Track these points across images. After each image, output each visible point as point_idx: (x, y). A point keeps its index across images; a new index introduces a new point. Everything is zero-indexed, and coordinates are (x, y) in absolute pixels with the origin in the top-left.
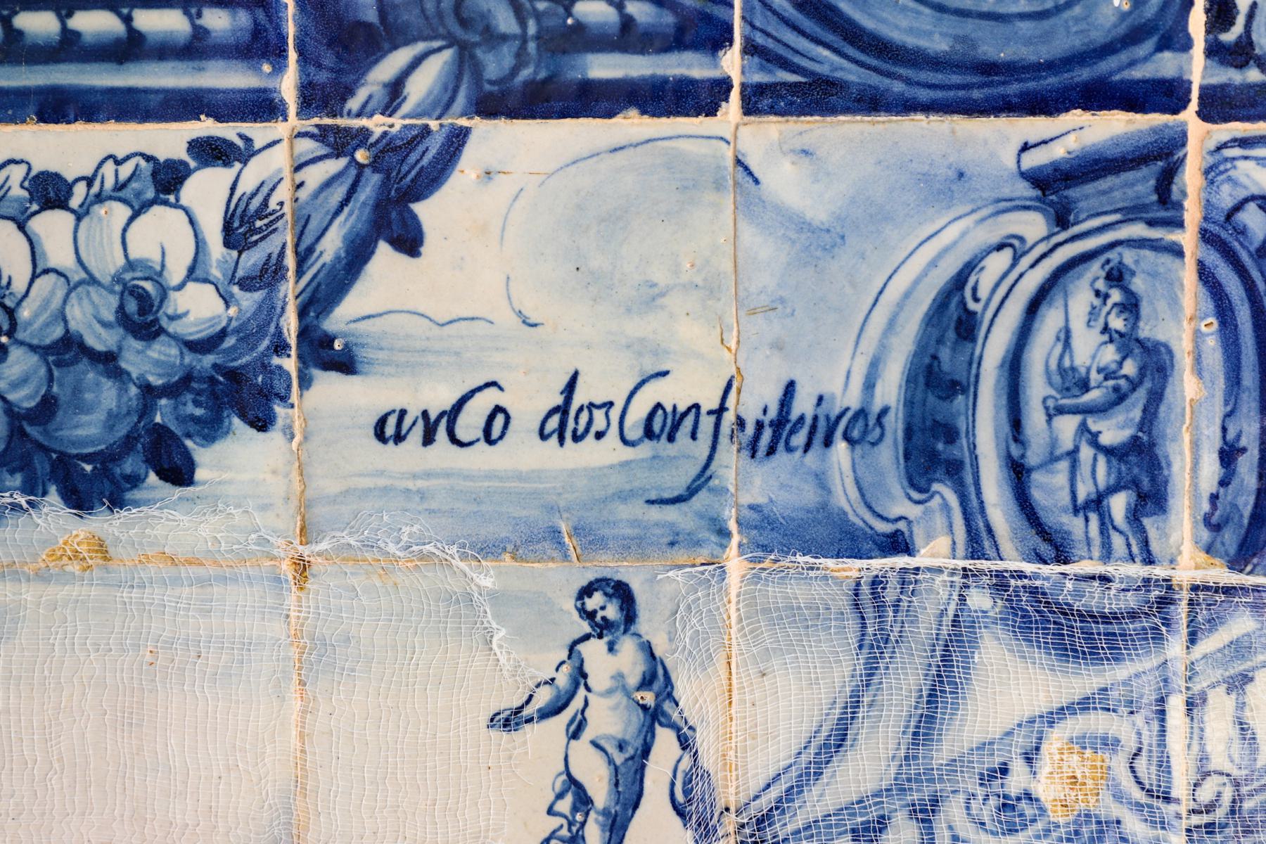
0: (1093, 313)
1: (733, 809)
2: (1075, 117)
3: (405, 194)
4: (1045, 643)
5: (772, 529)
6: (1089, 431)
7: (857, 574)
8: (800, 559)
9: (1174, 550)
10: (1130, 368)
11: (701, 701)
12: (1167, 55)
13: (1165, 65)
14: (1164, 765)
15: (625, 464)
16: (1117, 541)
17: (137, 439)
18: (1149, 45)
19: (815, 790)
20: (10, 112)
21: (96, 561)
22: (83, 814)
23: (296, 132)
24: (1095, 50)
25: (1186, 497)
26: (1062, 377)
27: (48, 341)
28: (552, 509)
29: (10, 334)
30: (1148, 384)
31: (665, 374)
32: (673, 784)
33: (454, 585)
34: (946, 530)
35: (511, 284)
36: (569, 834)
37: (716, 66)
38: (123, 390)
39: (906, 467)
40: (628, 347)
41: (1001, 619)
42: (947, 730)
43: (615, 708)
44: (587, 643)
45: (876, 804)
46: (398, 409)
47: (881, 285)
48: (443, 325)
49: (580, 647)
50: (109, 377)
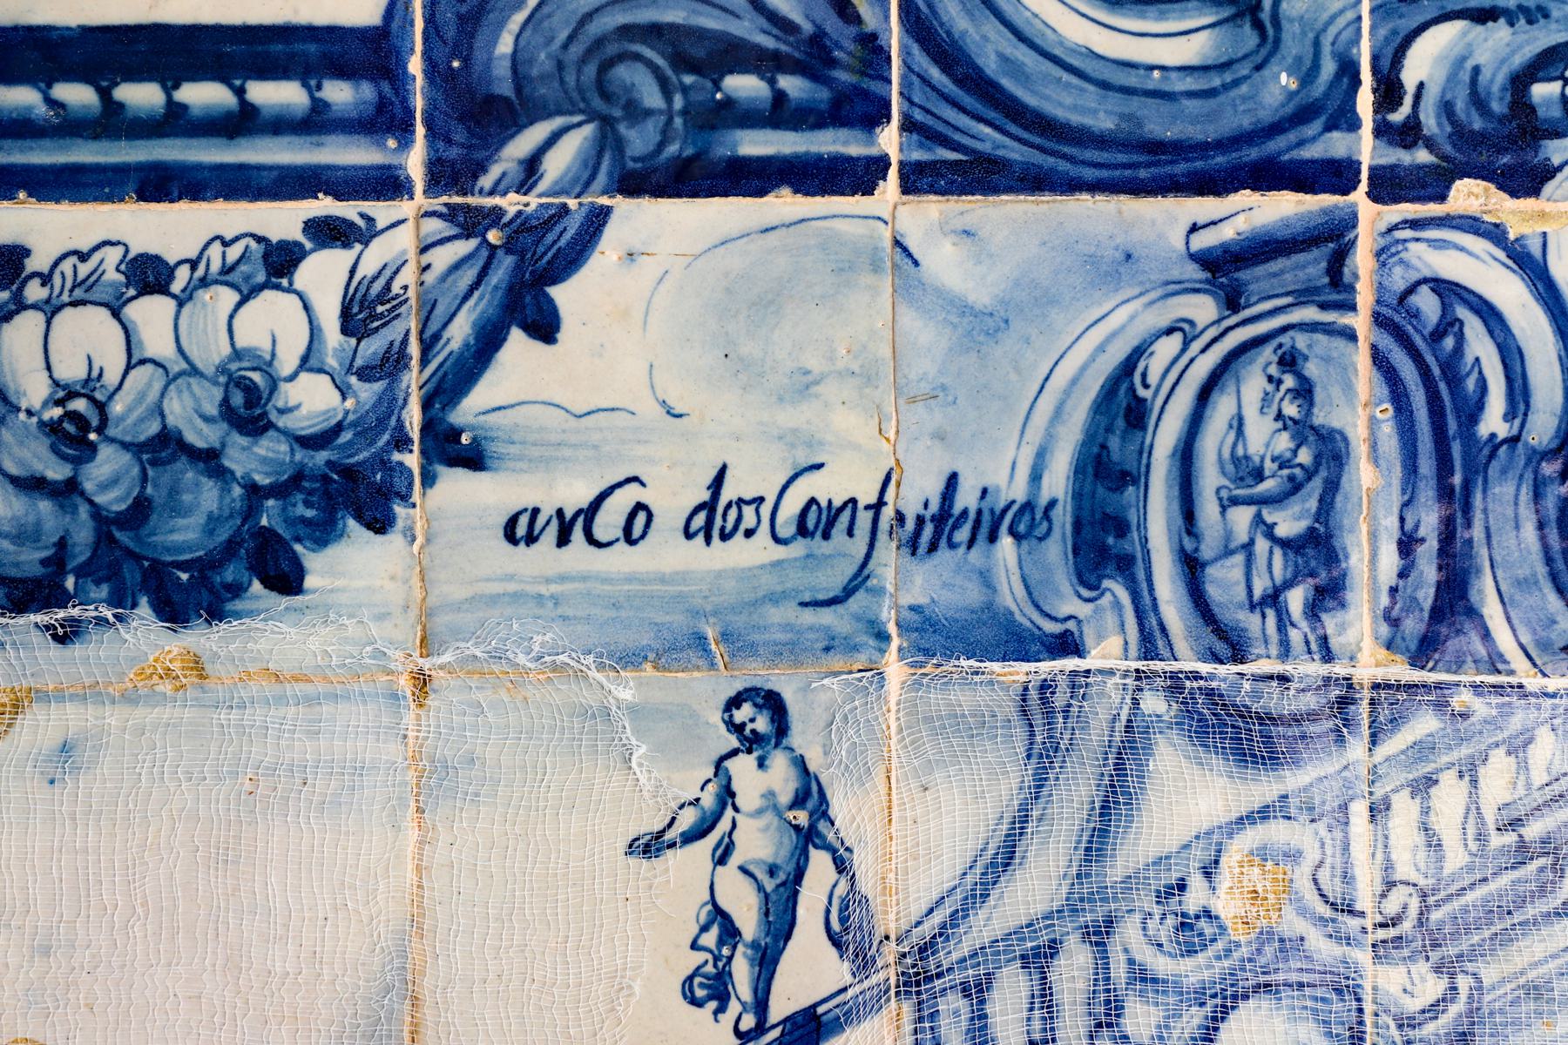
0: (1266, 399)
1: (893, 937)
2: (1244, 198)
3: (541, 276)
4: (1223, 748)
5: (935, 632)
6: (1264, 523)
7: (1024, 678)
8: (964, 663)
9: (1353, 647)
10: (1305, 456)
11: (858, 819)
12: (1335, 135)
13: (1335, 145)
14: (1347, 878)
15: (777, 564)
16: (1295, 636)
17: (240, 544)
18: (1316, 126)
19: (982, 914)
20: (107, 190)
21: (190, 680)
22: (169, 965)
23: (422, 211)
24: (1263, 129)
25: (1365, 591)
26: (1236, 467)
27: (142, 438)
28: (696, 613)
29: (100, 430)
30: (1323, 473)
31: (819, 466)
32: (828, 912)
33: (589, 698)
34: (1117, 629)
35: (654, 372)
36: (714, 971)
37: (871, 141)
38: (226, 490)
39: (1075, 563)
40: (780, 438)
41: (1177, 724)
42: (1122, 844)
43: (766, 829)
44: (735, 759)
45: (1047, 927)
46: (530, 508)
47: (1047, 371)
48: (580, 416)
49: (728, 764)
50: (210, 477)
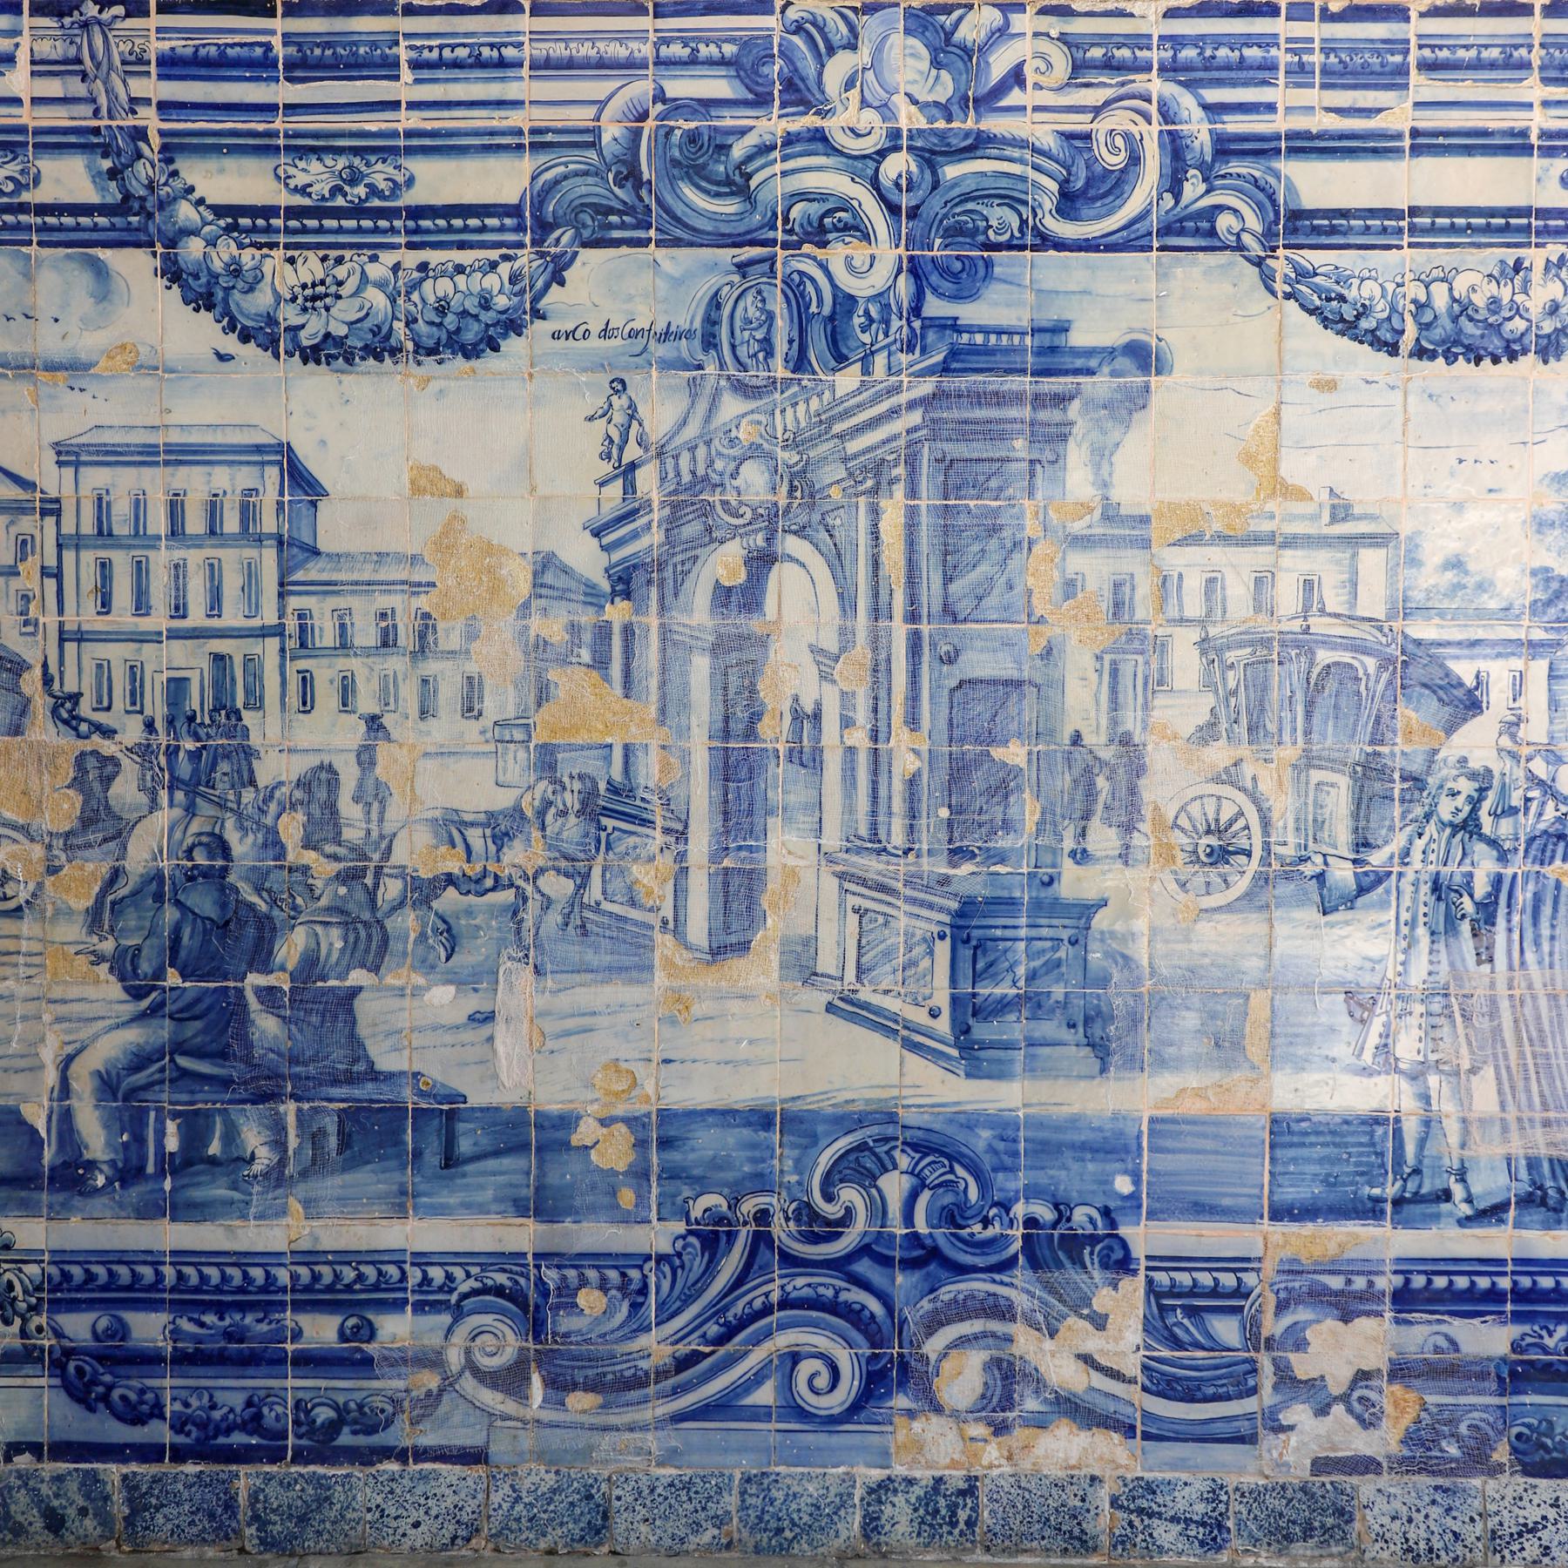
13: (771, 234)
